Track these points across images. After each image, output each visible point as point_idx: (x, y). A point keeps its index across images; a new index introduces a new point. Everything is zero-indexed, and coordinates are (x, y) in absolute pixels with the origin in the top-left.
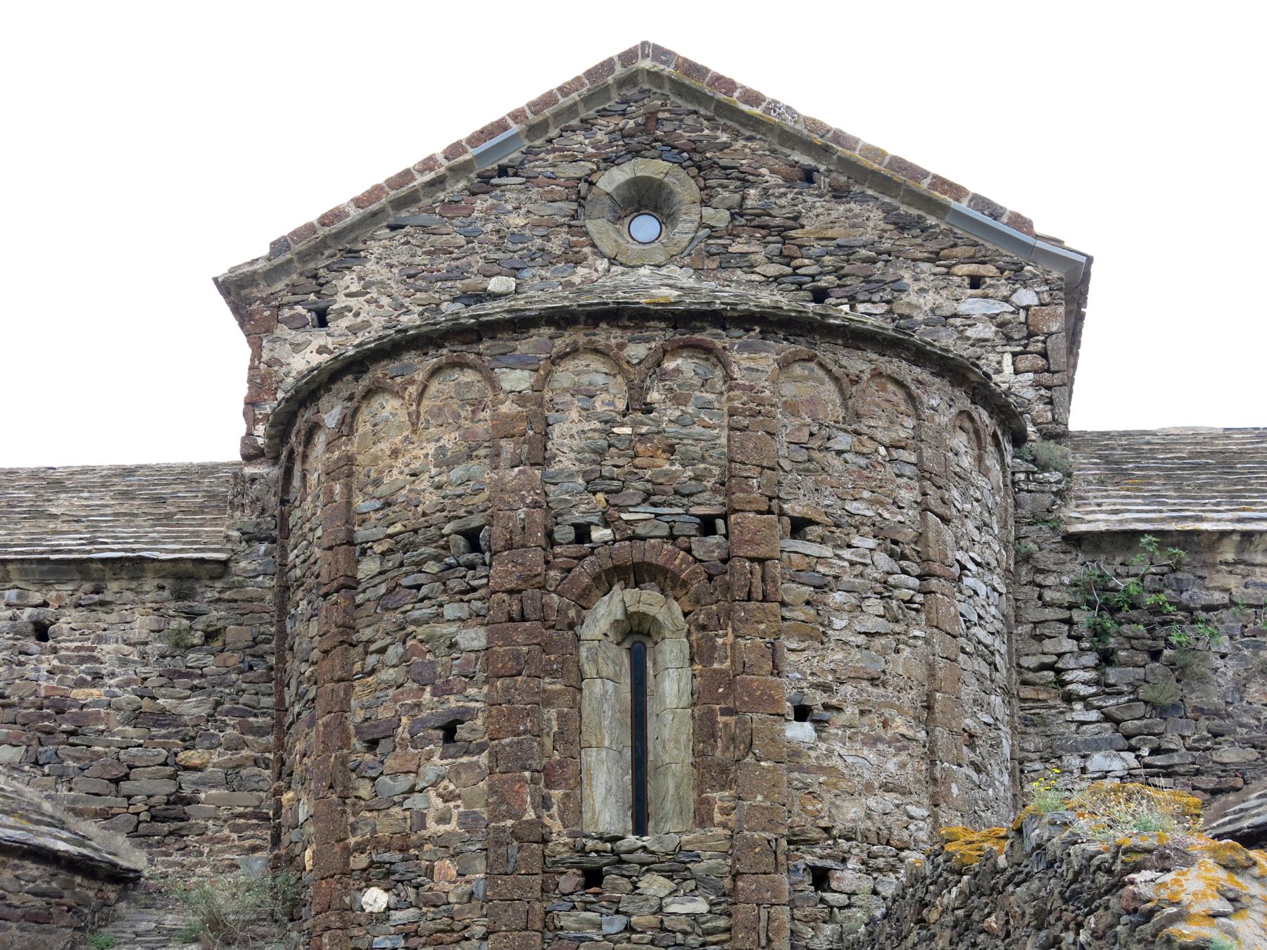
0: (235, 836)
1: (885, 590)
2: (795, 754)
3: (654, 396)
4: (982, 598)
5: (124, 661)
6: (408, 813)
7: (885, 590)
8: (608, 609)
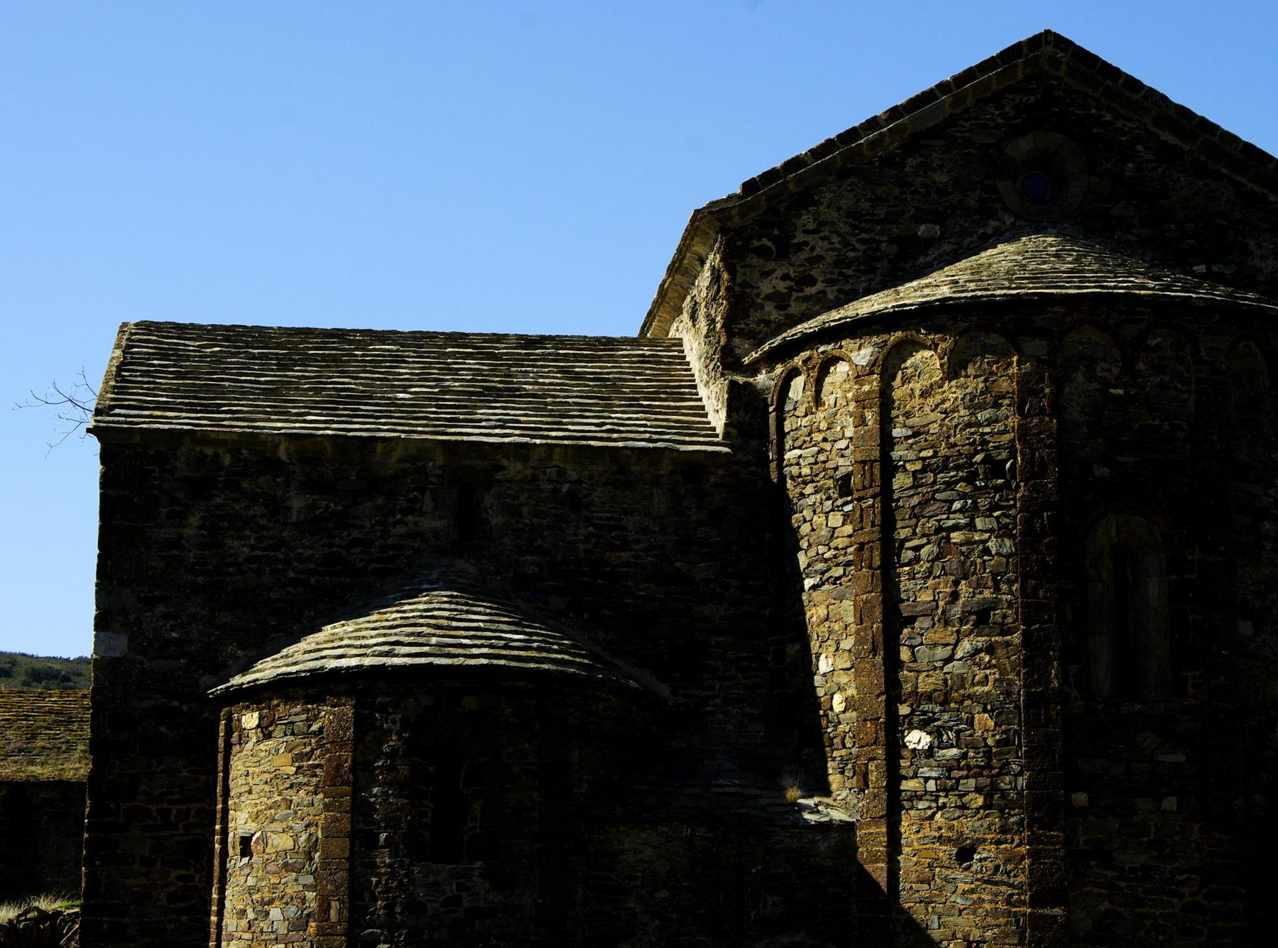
0: (740, 675)
3: (1141, 366)
5: (645, 531)
6: (948, 676)
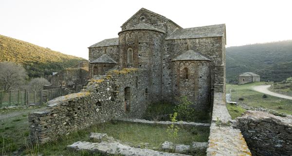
1: (146, 47)
2: (138, 58)
4: (157, 46)
7: (146, 47)
8: (129, 49)
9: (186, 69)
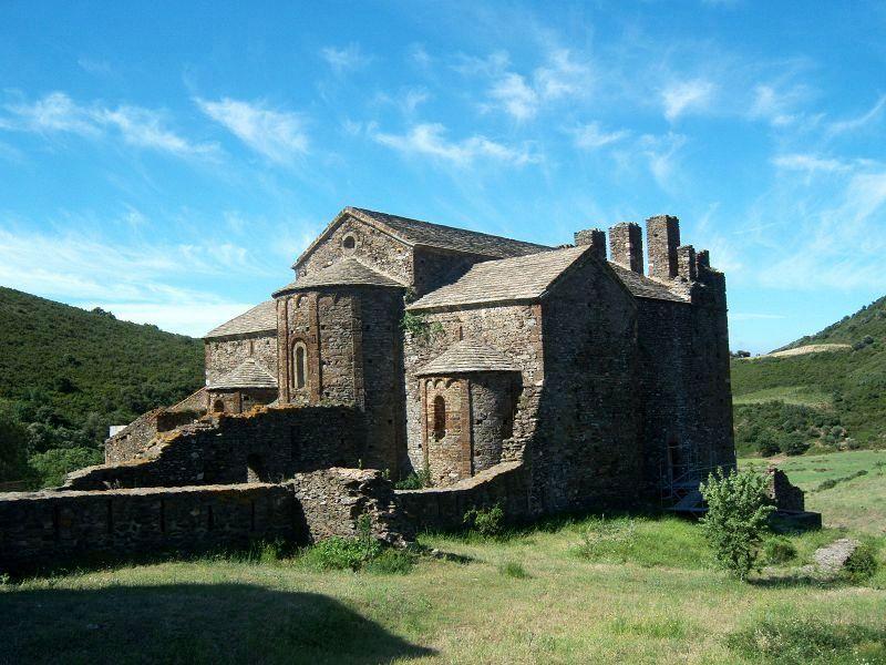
8: (300, 344)
9: (439, 401)
